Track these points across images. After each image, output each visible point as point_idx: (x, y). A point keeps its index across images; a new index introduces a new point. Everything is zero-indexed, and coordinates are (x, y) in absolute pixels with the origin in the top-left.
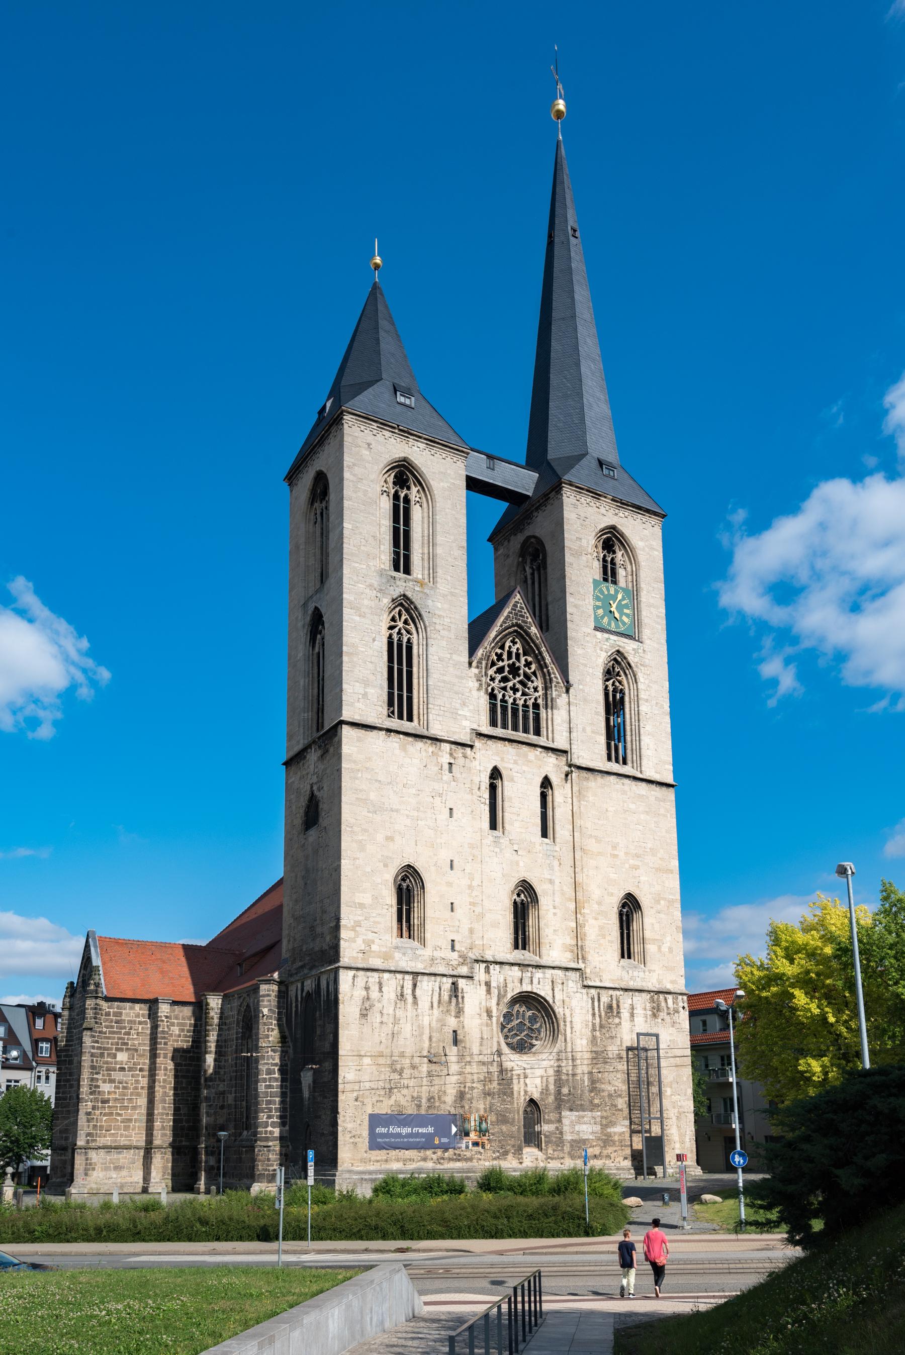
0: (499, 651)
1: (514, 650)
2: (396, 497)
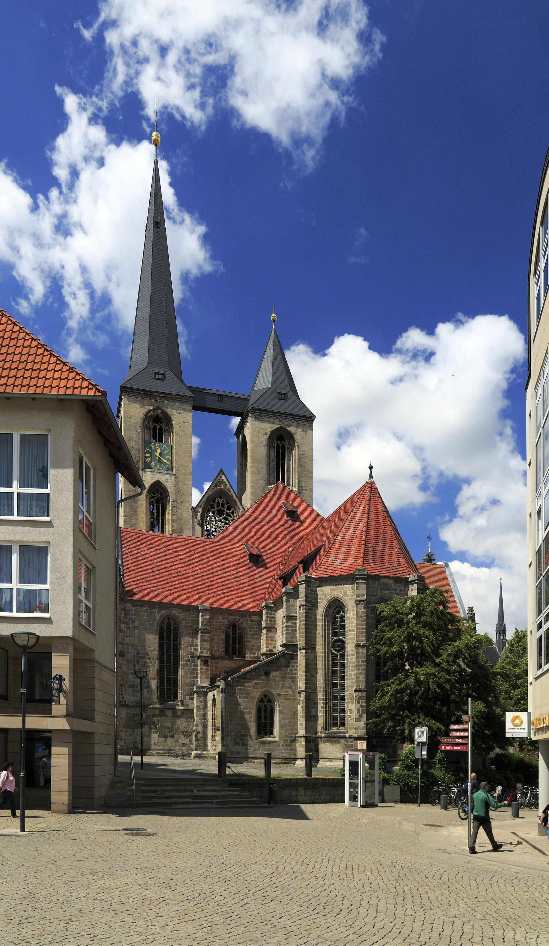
0: (212, 503)
1: (221, 502)
2: (155, 428)
